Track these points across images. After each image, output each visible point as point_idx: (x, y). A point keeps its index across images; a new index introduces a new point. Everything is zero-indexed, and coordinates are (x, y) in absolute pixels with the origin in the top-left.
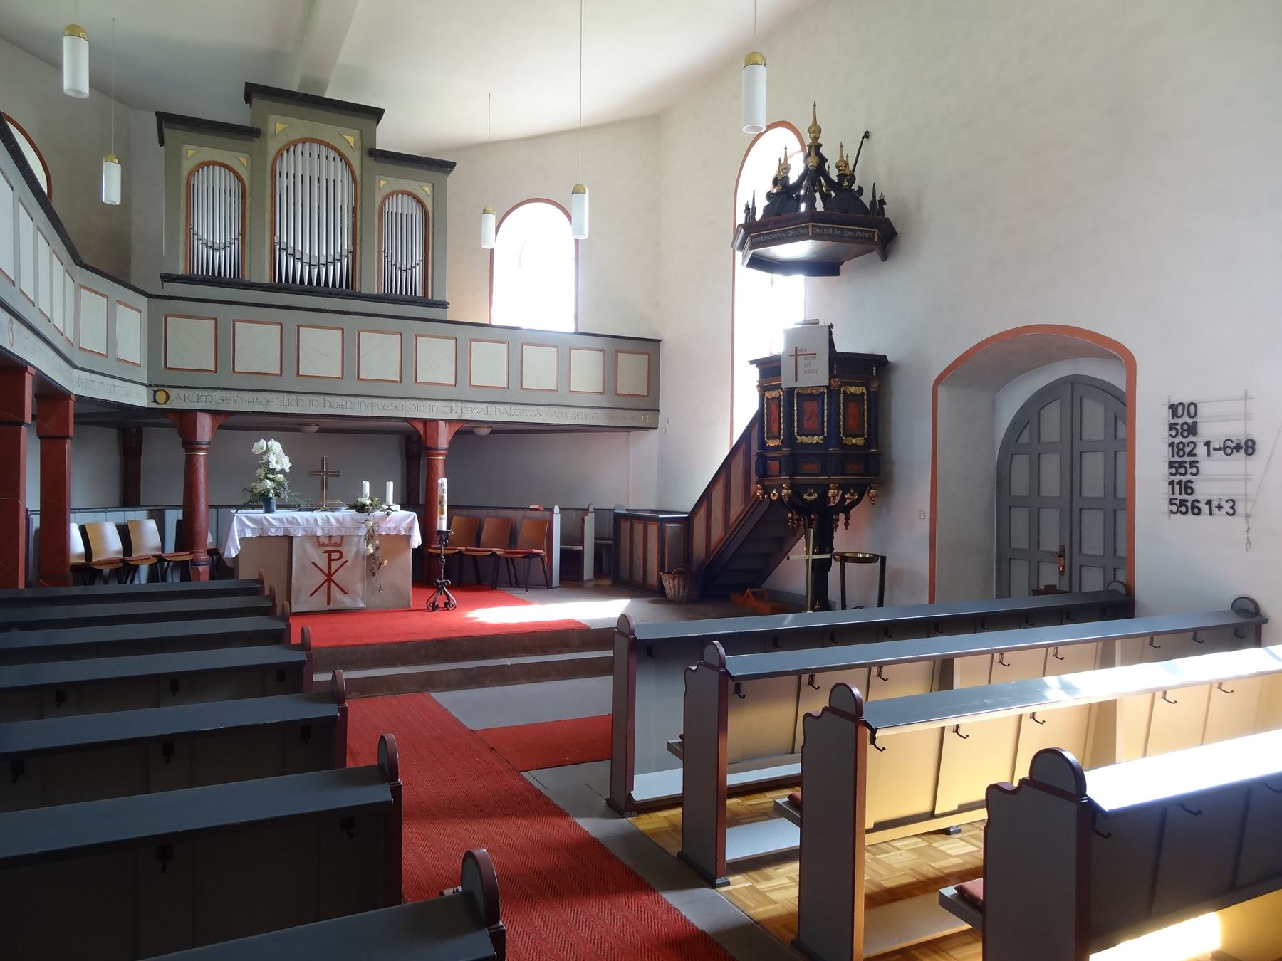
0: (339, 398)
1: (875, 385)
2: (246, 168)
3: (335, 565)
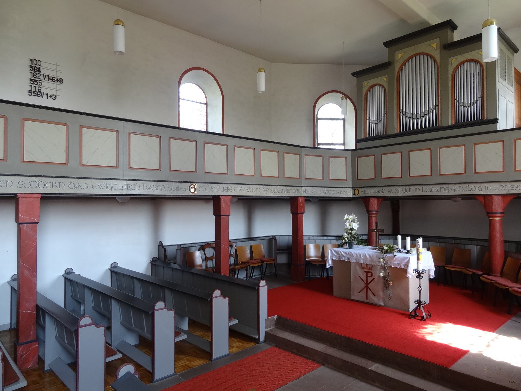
0: (430, 186)
2: (386, 82)
3: (369, 279)
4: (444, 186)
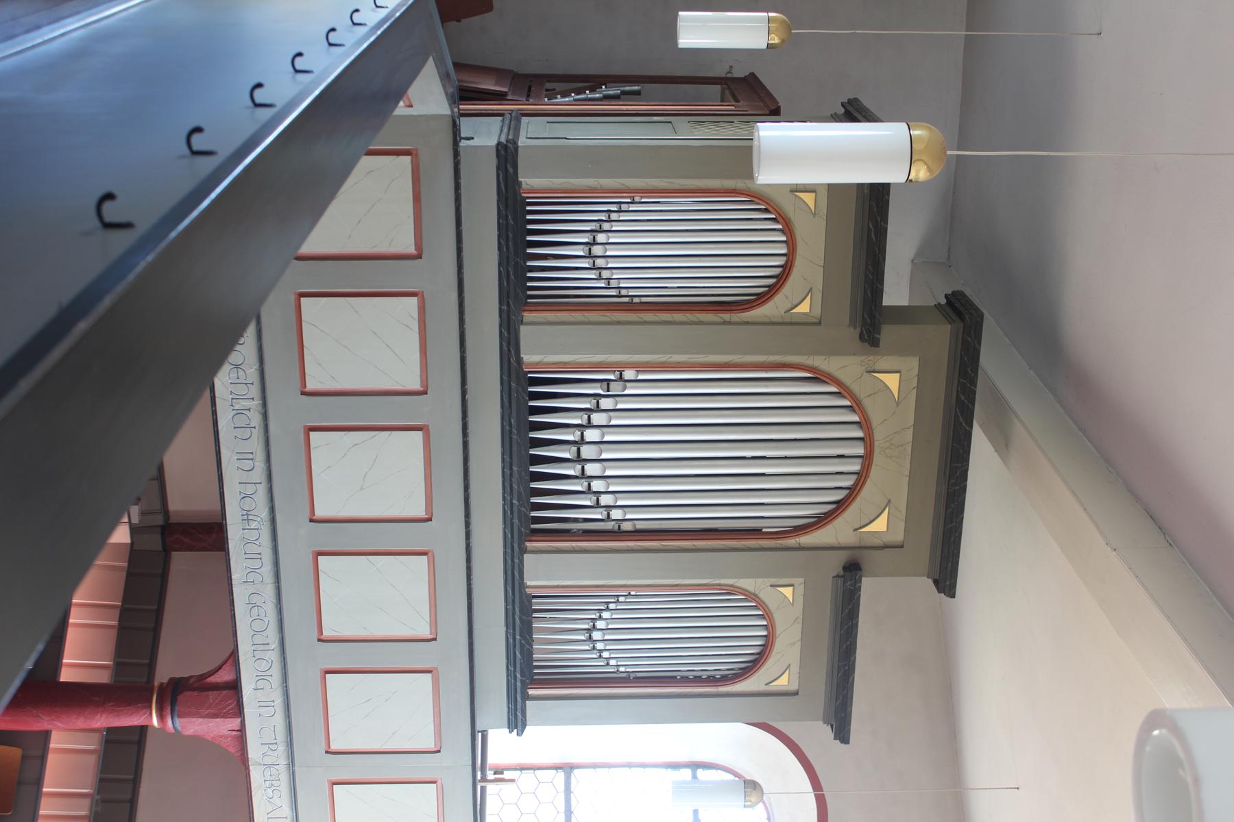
0: (264, 513)
4: (267, 568)
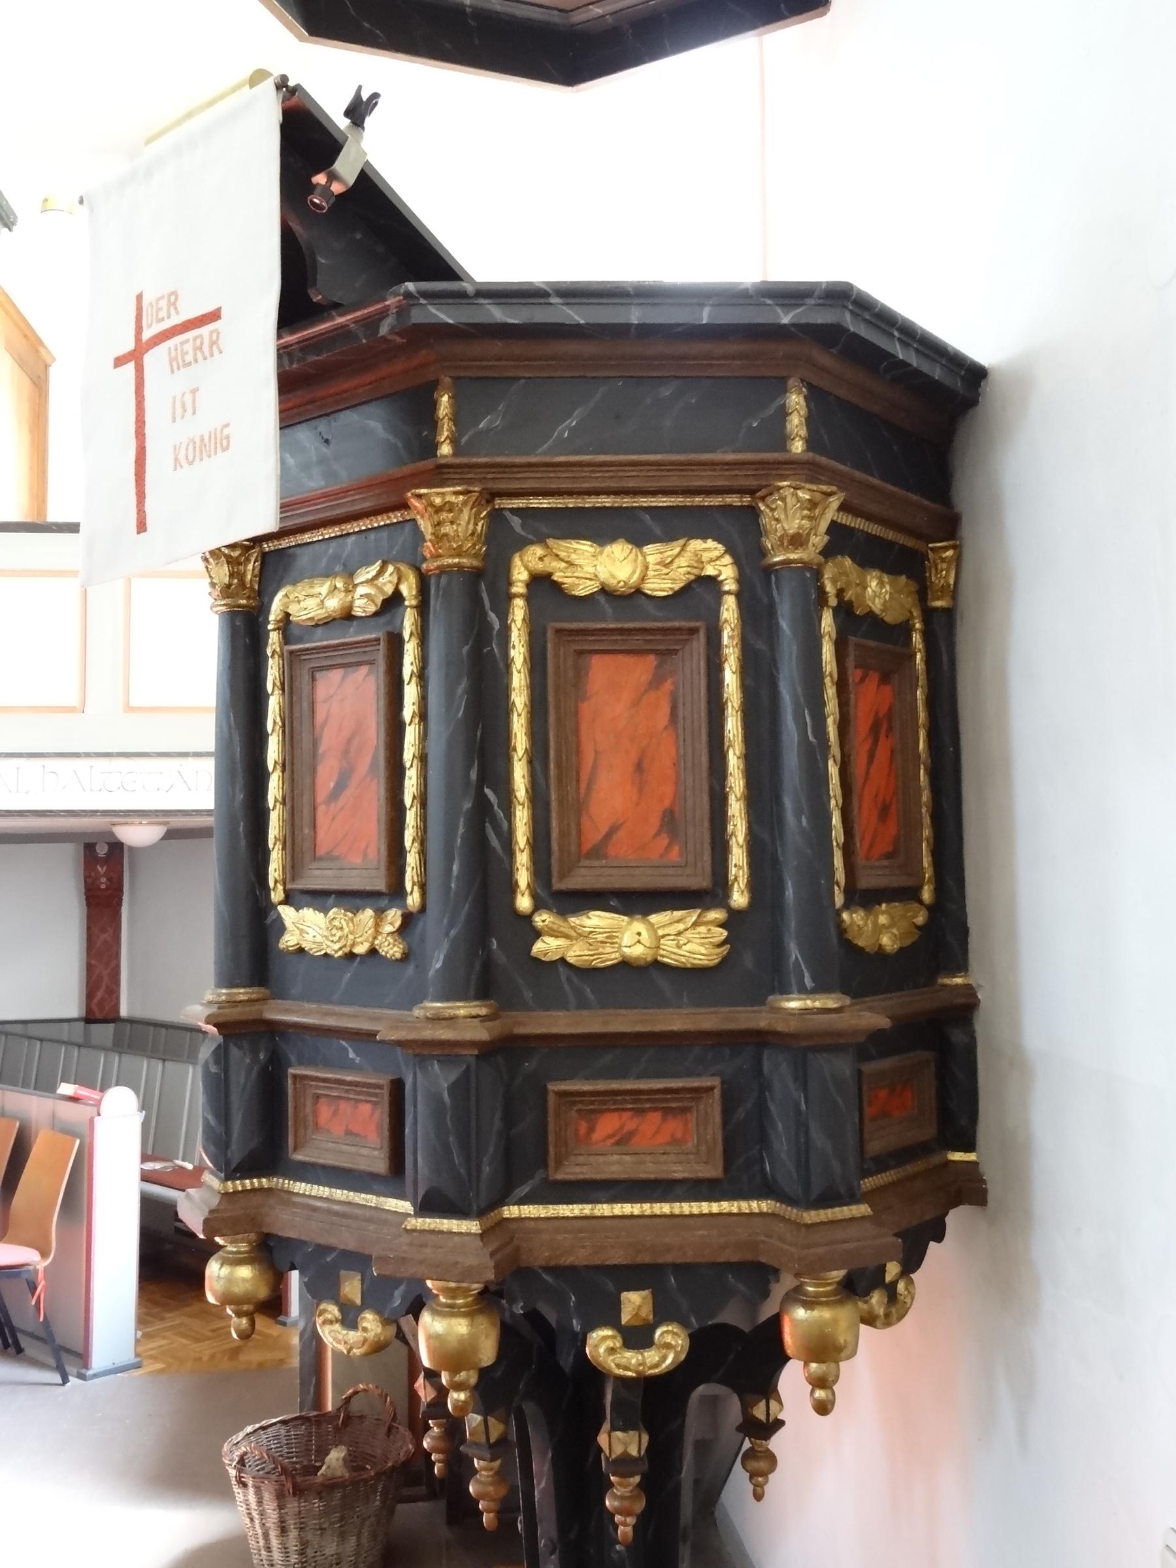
1: (794, 523)
